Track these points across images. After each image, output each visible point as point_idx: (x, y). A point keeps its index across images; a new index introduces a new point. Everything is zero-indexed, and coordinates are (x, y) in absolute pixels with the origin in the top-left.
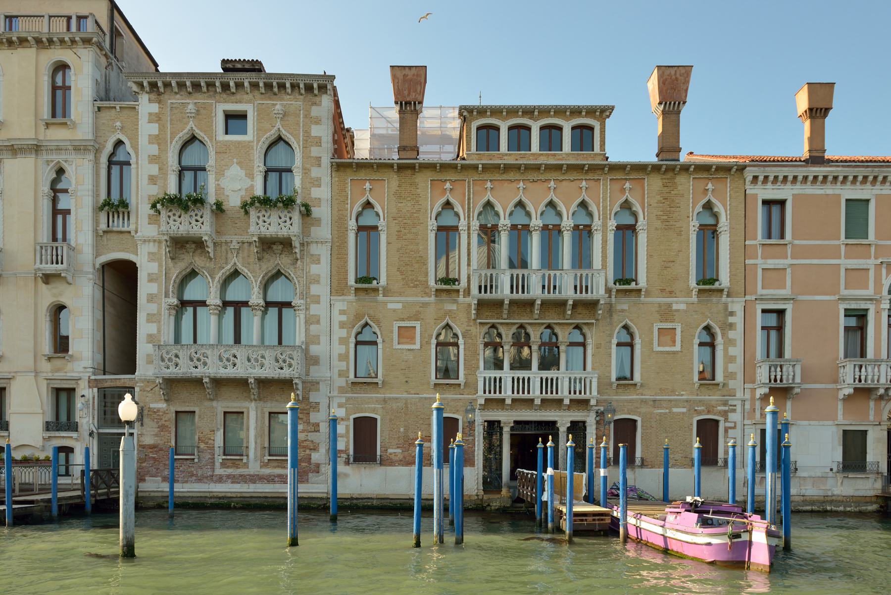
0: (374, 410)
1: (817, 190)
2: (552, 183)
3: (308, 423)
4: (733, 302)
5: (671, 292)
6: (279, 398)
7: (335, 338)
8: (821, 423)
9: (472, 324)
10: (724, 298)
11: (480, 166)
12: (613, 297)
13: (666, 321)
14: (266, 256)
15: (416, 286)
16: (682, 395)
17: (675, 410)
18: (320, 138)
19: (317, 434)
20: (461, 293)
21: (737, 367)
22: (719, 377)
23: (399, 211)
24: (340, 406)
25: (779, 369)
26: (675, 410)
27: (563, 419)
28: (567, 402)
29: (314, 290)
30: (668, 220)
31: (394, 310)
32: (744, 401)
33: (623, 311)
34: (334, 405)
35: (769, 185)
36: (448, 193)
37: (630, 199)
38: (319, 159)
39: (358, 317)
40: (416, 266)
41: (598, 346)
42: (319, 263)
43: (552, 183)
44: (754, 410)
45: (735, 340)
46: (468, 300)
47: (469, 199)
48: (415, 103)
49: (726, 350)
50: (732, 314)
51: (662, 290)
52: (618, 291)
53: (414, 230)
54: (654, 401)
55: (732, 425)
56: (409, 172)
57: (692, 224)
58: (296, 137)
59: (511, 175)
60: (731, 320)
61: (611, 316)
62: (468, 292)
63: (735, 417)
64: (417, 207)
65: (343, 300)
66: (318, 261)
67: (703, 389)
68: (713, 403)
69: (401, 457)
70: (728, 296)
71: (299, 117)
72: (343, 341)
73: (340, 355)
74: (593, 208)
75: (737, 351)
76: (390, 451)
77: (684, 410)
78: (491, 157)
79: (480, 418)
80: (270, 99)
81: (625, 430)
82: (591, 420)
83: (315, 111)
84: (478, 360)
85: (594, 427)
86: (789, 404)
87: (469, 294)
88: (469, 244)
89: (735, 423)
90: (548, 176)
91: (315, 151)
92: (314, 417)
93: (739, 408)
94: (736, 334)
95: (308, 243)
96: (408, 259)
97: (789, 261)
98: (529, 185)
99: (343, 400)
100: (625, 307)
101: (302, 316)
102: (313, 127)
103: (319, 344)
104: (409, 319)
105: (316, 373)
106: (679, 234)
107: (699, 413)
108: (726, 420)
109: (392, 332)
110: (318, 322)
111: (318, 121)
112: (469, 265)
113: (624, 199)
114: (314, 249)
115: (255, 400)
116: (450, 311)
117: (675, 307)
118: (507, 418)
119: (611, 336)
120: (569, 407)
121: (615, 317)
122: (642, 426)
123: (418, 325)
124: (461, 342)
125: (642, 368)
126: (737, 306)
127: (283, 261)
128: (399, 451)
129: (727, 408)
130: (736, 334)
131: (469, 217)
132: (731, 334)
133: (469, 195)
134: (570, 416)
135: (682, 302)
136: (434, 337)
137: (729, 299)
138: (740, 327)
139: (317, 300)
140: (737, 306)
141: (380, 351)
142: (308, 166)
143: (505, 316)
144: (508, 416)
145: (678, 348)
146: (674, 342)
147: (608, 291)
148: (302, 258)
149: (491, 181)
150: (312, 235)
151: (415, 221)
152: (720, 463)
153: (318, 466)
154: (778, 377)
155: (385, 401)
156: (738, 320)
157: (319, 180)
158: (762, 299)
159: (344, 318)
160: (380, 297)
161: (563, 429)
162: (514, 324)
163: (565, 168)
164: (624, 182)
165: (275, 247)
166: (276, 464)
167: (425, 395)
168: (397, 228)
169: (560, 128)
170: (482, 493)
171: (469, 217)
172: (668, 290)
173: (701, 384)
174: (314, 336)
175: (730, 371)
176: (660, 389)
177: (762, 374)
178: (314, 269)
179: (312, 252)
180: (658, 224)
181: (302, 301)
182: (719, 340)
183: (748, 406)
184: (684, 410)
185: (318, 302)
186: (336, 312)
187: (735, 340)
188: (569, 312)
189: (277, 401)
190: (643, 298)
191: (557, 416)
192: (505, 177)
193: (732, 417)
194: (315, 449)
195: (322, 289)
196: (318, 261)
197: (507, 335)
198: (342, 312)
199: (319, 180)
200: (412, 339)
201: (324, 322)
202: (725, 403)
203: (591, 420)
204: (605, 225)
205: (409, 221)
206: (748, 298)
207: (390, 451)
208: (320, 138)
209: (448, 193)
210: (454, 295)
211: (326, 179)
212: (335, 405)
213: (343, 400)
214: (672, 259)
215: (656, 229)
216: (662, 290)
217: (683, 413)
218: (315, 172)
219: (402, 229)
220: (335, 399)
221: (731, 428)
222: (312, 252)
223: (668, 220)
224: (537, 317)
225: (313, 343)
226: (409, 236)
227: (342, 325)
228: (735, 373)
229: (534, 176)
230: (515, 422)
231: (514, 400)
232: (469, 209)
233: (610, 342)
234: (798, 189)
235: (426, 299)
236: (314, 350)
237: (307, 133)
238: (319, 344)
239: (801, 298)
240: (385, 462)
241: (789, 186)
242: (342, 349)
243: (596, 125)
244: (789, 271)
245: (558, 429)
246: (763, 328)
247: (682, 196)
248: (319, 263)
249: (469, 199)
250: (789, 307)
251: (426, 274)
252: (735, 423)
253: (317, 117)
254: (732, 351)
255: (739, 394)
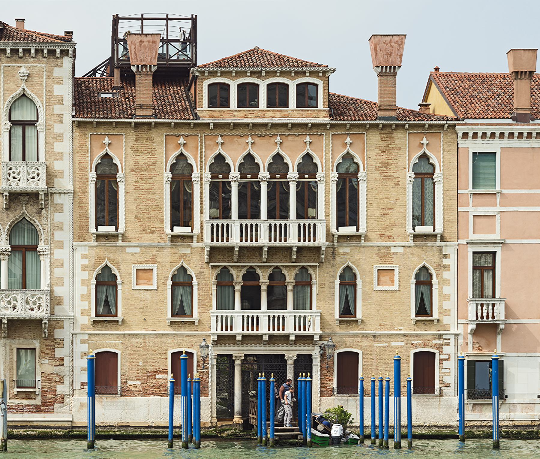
0: (114, 346)
1: (523, 144)
2: (278, 138)
3: (53, 357)
4: (446, 246)
5: (389, 237)
6: (26, 335)
7: (78, 280)
8: (529, 354)
9: (205, 266)
10: (438, 243)
11: (212, 124)
12: (335, 242)
13: (385, 262)
14: (14, 206)
15: (152, 232)
16: (400, 330)
17: (393, 344)
18: (62, 97)
19: (62, 367)
20: (195, 239)
21: (451, 305)
22: (435, 315)
23: (137, 163)
24: (83, 342)
25: (490, 307)
26: (393, 344)
27: (291, 353)
28: (292, 338)
29: (58, 236)
30: (385, 171)
31: (133, 254)
32: (457, 336)
33: (345, 254)
34: (77, 340)
35: (479, 140)
36: (182, 147)
37: (351, 152)
38: (61, 116)
39: (99, 260)
40: (153, 213)
41: (322, 286)
42: (62, 212)
43: (278, 138)
44: (467, 343)
45: (449, 280)
46: (201, 245)
47: (201, 153)
48: (150, 66)
49: (440, 289)
50: (445, 256)
51: (382, 235)
52: (340, 237)
53: (150, 181)
54: (374, 336)
55: (447, 357)
56: (146, 128)
57: (408, 174)
58: (40, 96)
59: (240, 132)
60: (445, 261)
61: (334, 258)
62: (200, 238)
63: (449, 350)
64: (153, 160)
65: (85, 246)
66: (61, 210)
67: (419, 324)
68: (429, 338)
69: (140, 388)
70: (442, 239)
71: (42, 77)
72: (84, 283)
73: (82, 296)
74: (317, 160)
75: (451, 290)
76: (130, 383)
77: (402, 344)
78: (221, 114)
79: (213, 353)
80: (16, 62)
81: (348, 363)
82: (316, 353)
83: (57, 72)
84: (211, 299)
85: (319, 359)
86: (499, 338)
87: (202, 239)
88: (201, 193)
89: (449, 355)
90: (275, 131)
91: (57, 109)
92: (59, 352)
93: (452, 341)
94: (450, 275)
95: (52, 194)
96: (144, 207)
97: (499, 208)
98: (257, 140)
99: (86, 337)
100: (347, 250)
101: (47, 260)
102: (55, 86)
103: (63, 285)
104: (147, 262)
105: (59, 312)
106: (397, 184)
107: (416, 347)
108: (441, 352)
109: (130, 274)
110: (62, 265)
111: (60, 81)
112: (201, 213)
113: (345, 152)
114: (58, 199)
115: (4, 337)
116: (185, 254)
117: (393, 250)
118: (237, 352)
119: (334, 276)
120: (295, 342)
121: (338, 259)
122: (363, 358)
123: (154, 267)
124: (195, 282)
125: (363, 306)
126: (451, 251)
127: (29, 211)
128: (138, 382)
129: (441, 342)
130: (450, 275)
131: (201, 169)
132: (445, 275)
133: (201, 149)
134: (297, 350)
135: (399, 246)
136: (170, 278)
137: (443, 243)
138: (454, 268)
139: (60, 245)
140: (451, 251)
141: (119, 293)
142: (51, 123)
143: (236, 259)
144: (239, 350)
145: (396, 287)
146: (393, 281)
147: (329, 236)
148: (46, 207)
149: (222, 136)
150: (56, 186)
151: (152, 173)
152: (437, 391)
153: (63, 397)
154: (490, 315)
155: (124, 336)
156: (451, 261)
157: (61, 135)
158: (473, 244)
159: (86, 262)
160: (120, 243)
161: (290, 362)
162: (244, 266)
163: (290, 125)
164: (345, 136)
165: (22, 198)
166: (24, 396)
167: (162, 332)
168: (135, 179)
169: (286, 87)
170: (215, 420)
171: (201, 169)
172: (387, 234)
173: (417, 321)
174: (58, 278)
175: (444, 308)
176: (380, 325)
177: (471, 311)
178: (58, 217)
179: (55, 202)
180: (377, 175)
181: (47, 247)
182: (435, 280)
183: (461, 341)
184: (402, 344)
185: (62, 247)
186: (78, 255)
187: (449, 280)
188: (295, 257)
189: (24, 338)
190: (363, 243)
191: (284, 350)
192: (234, 132)
193: (446, 349)
194: (61, 382)
195: (65, 236)
196: (61, 210)
197: (238, 276)
198: (84, 256)
199: (61, 135)
200: (149, 280)
201: (67, 265)
202: (440, 336)
203: (316, 353)
204: (327, 177)
205: (146, 173)
206: (460, 242)
207: (130, 383)
208: (62, 97)
209: (182, 147)
210: (188, 240)
211: (68, 135)
212: (79, 342)
213: (86, 337)
214: (390, 207)
215: (375, 179)
216: (382, 235)
217: (401, 346)
218: (57, 128)
219: (139, 180)
220: (78, 336)
221: (445, 360)
222: (55, 202)
223: (385, 171)
224: (265, 260)
225: (57, 285)
226: (146, 186)
227: (84, 268)
228: (450, 310)
229: (263, 132)
230: (246, 355)
231: (243, 336)
232: (201, 161)
233: (334, 282)
234: (506, 143)
235: (163, 244)
236: (58, 291)
237: (50, 92)
238: (63, 285)
239: (508, 241)
240: (125, 393)
241: (497, 140)
242: (85, 290)
243: (320, 83)
244: (498, 217)
245: (286, 361)
246: (475, 268)
247: (400, 149)
248: (62, 212)
249: (201, 153)
250: (498, 250)
251: (162, 222)
252: (449, 355)
253: (59, 78)
254: (446, 290)
255: (454, 330)
